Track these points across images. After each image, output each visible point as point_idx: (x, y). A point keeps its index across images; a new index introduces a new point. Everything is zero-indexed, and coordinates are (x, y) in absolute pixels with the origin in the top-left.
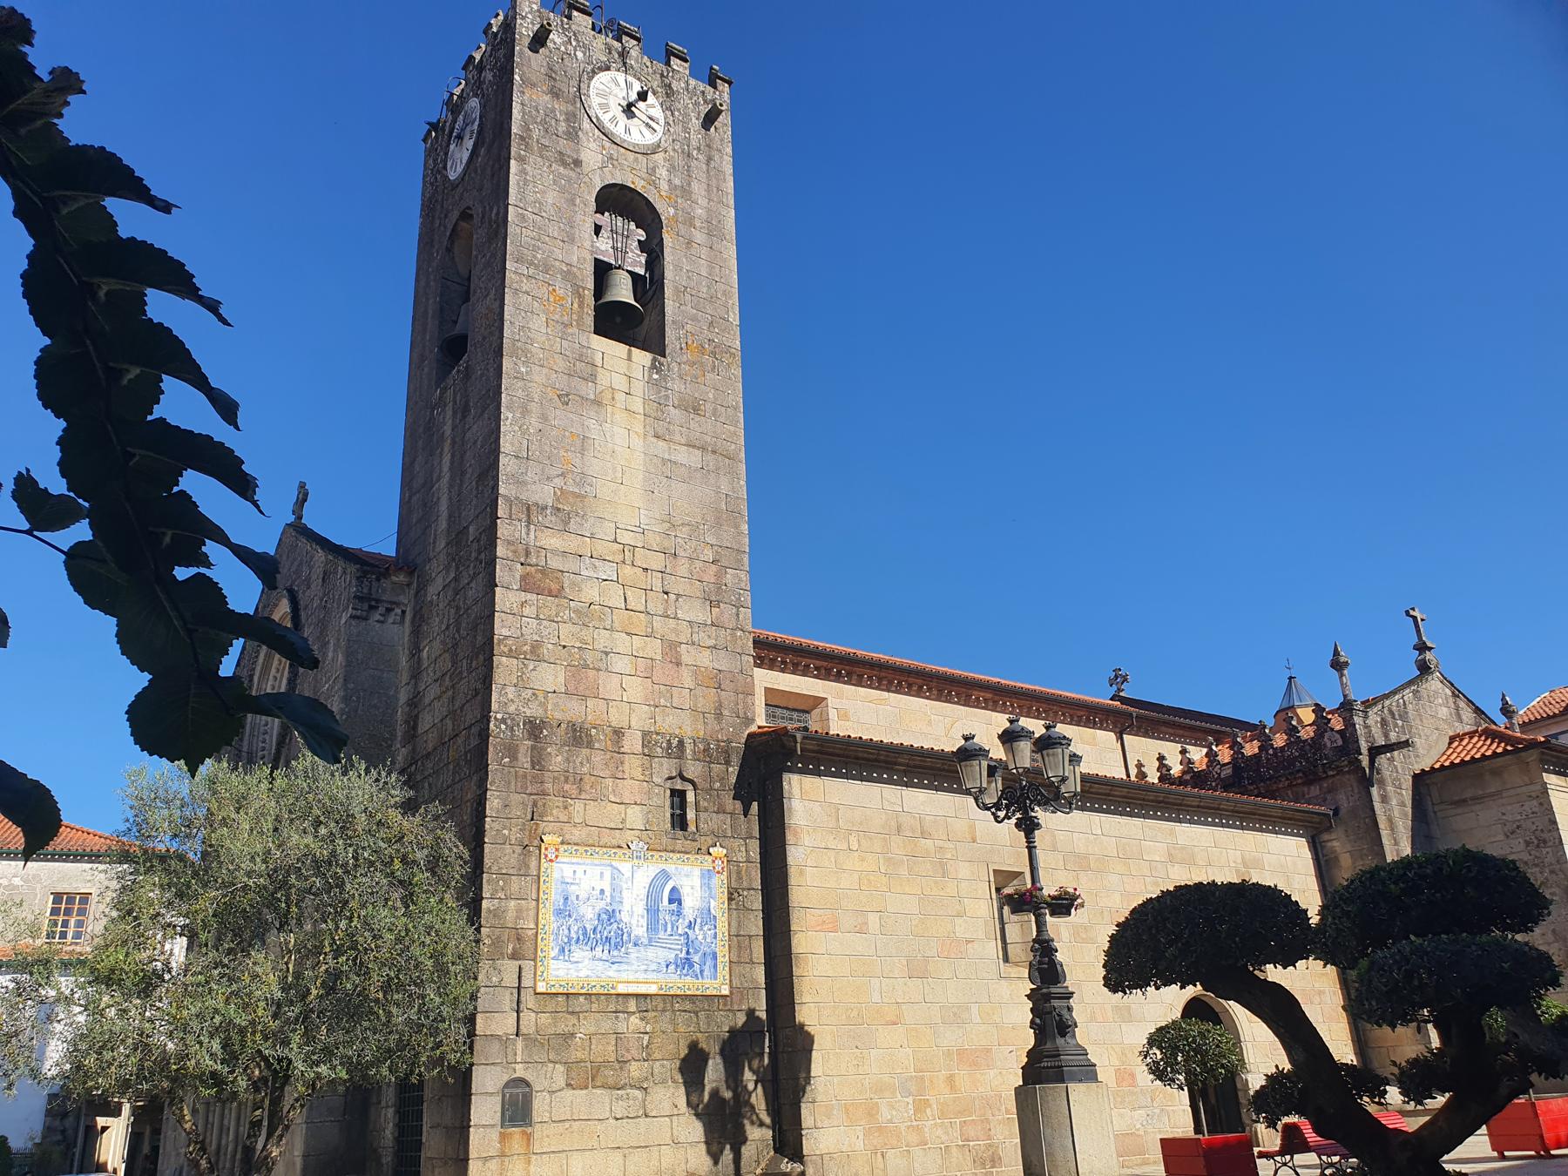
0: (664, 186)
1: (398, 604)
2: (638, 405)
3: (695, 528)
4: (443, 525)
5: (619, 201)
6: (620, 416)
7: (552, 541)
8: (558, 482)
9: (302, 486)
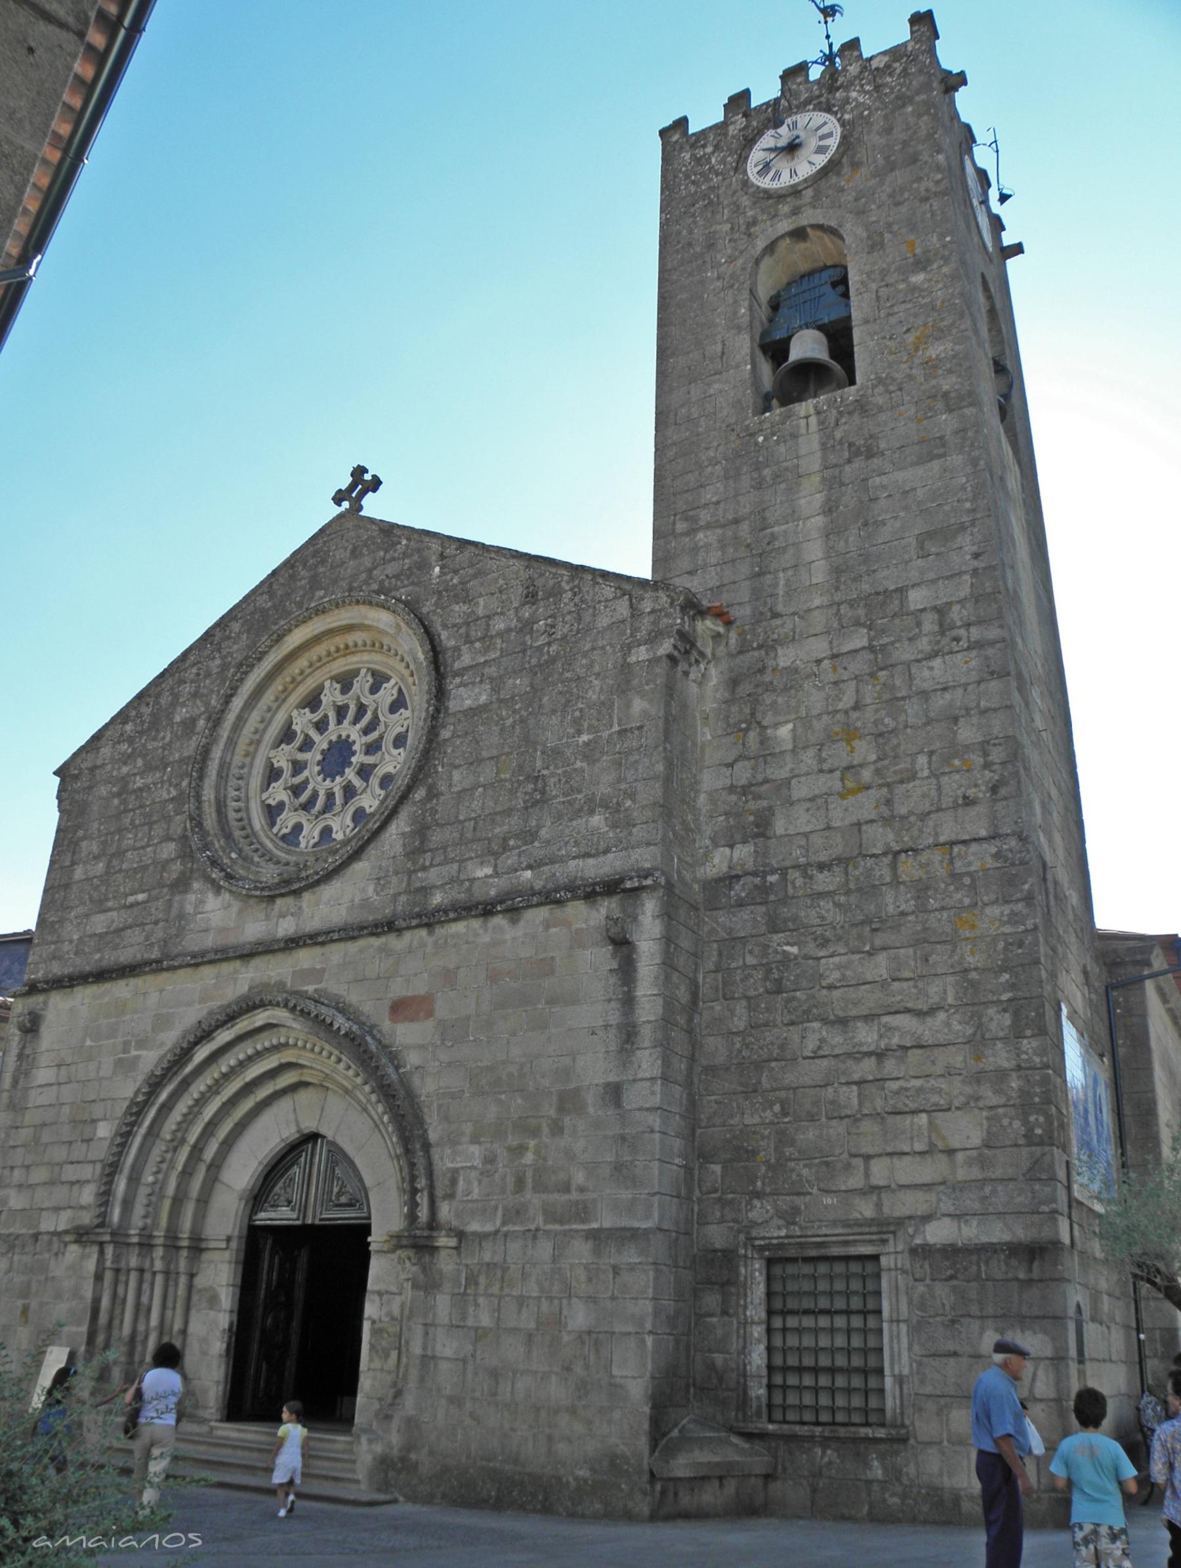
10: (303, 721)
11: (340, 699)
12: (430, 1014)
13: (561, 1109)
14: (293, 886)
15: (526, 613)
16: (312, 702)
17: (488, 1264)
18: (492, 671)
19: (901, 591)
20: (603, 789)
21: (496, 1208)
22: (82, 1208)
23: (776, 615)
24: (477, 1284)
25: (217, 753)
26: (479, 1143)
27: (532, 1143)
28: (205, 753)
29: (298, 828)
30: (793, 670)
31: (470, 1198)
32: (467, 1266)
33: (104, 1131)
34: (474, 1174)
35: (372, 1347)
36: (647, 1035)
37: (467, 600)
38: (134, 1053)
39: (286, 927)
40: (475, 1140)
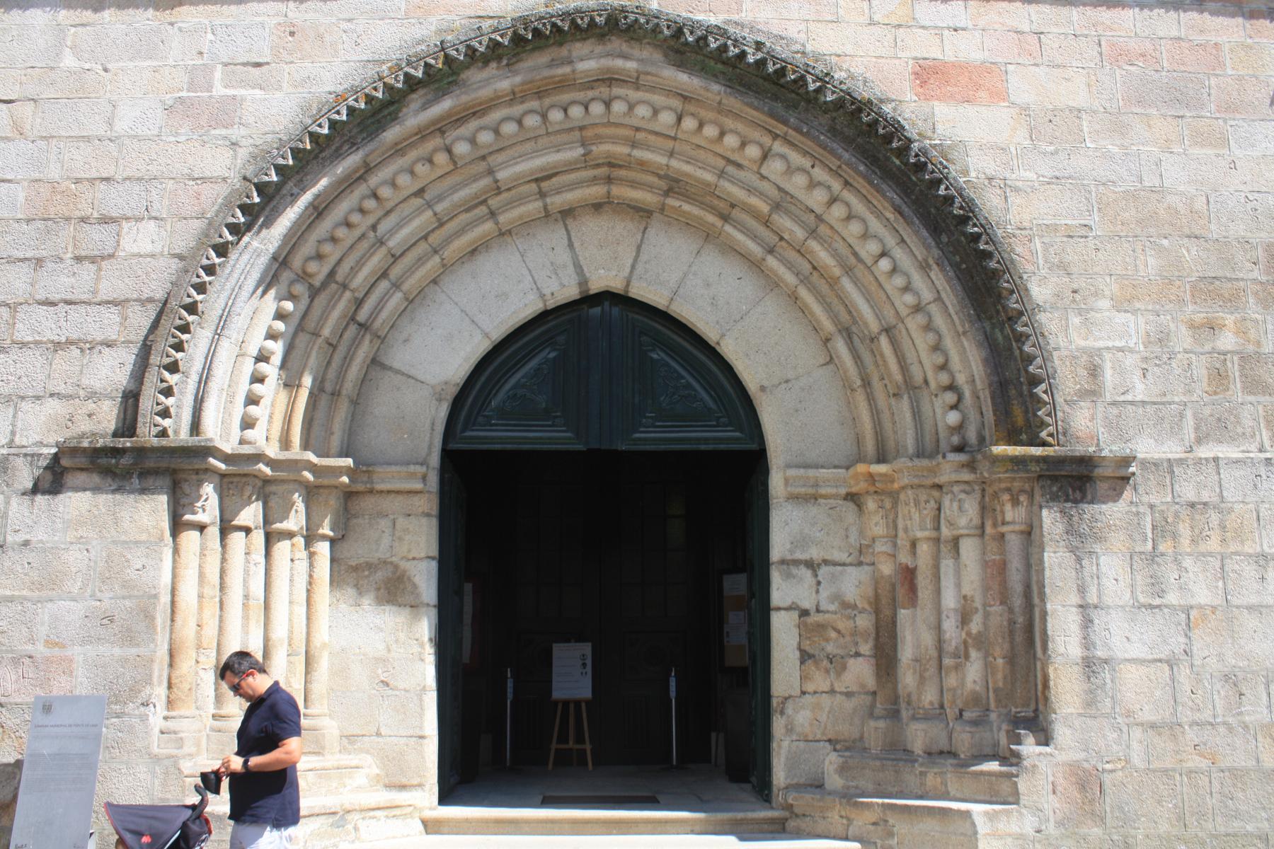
12: (999, 95)
17: (1192, 505)
21: (1182, 416)
22: (93, 395)
24: (1175, 536)
26: (1135, 312)
27: (1230, 319)
31: (1129, 397)
32: (1152, 507)
34: (1130, 361)
35: (805, 656)
38: (219, 90)
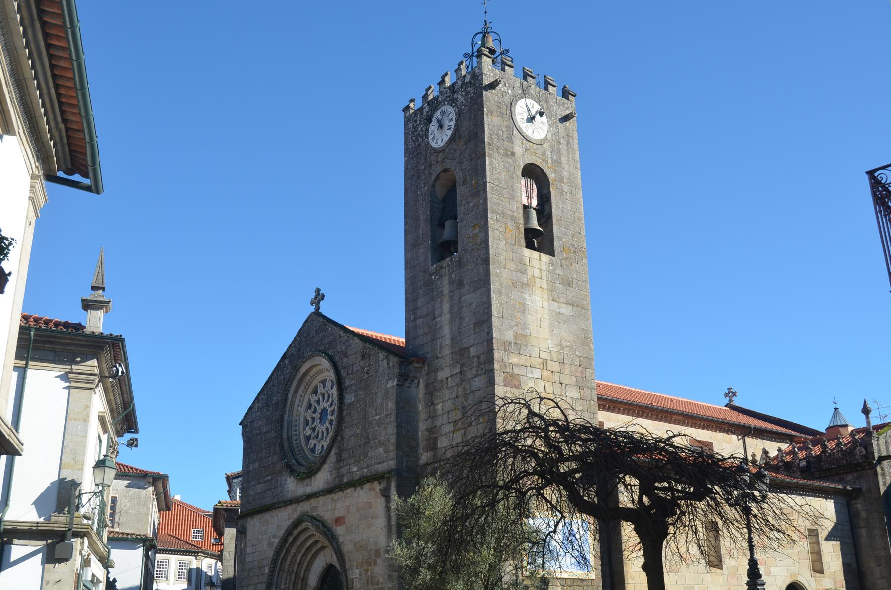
0: (550, 161)
1: (416, 377)
2: (545, 285)
3: (571, 348)
4: (447, 341)
5: (532, 172)
6: (538, 291)
7: (515, 360)
8: (515, 329)
9: (318, 290)
10: (314, 398)
11: (316, 398)
13: (376, 556)
14: (311, 473)
15: (362, 364)
16: (315, 392)
18: (354, 387)
19: (468, 348)
20: (382, 438)
23: (437, 358)
25: (286, 418)
28: (282, 417)
29: (315, 445)
30: (441, 381)
33: (267, 570)
36: (394, 529)
37: (347, 357)
39: (309, 490)
40: (357, 568)
